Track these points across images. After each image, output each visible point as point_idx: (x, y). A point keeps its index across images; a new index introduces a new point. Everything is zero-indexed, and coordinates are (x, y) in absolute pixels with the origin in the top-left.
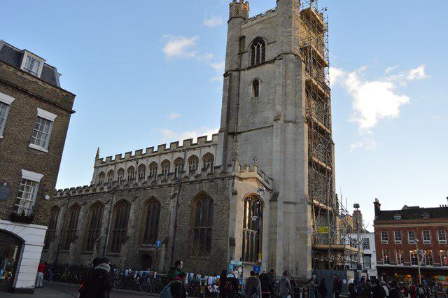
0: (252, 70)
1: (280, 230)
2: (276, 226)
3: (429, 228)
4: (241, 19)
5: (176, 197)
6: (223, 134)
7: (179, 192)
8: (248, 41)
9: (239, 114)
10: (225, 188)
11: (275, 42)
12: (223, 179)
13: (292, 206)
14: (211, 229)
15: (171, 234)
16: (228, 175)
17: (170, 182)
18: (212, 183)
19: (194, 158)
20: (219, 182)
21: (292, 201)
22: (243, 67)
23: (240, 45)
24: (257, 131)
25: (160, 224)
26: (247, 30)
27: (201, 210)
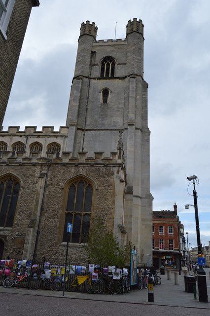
0: (102, 81)
1: (133, 219)
2: (131, 216)
5: (45, 178)
6: (74, 128)
7: (48, 172)
8: (99, 58)
9: (89, 113)
11: (125, 64)
14: (89, 215)
15: (38, 218)
16: (111, 162)
17: (34, 161)
18: (92, 168)
19: (37, 147)
20: (103, 170)
21: (140, 196)
23: (91, 57)
25: (19, 204)
27: (76, 194)
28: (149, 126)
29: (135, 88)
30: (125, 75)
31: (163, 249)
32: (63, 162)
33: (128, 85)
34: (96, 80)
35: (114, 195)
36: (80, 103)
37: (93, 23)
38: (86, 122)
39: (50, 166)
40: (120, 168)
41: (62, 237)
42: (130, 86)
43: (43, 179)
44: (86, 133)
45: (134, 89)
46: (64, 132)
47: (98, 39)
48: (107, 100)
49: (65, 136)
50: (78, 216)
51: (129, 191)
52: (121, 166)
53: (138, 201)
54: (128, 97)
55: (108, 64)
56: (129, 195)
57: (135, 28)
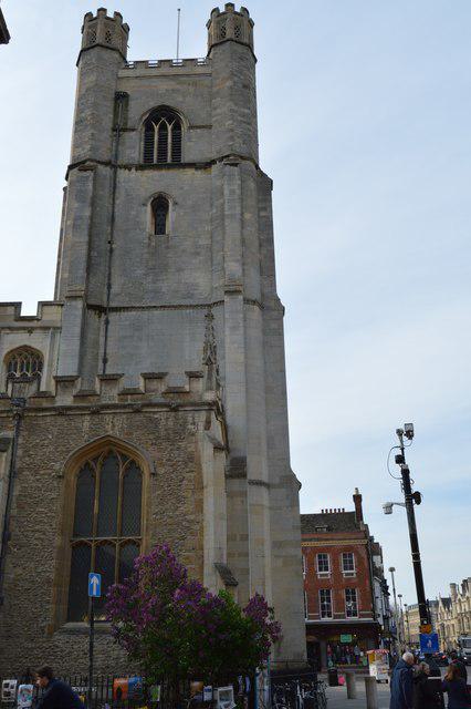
0: (149, 173)
1: (251, 545)
2: (245, 538)
3: (328, 549)
4: (117, 55)
6: (79, 304)
8: (137, 111)
9: (117, 262)
10: (181, 433)
12: (175, 410)
13: (264, 490)
18: (138, 417)
20: (164, 418)
21: (265, 479)
22: (119, 163)
24: (166, 312)
26: (133, 83)
27: (97, 490)
28: (280, 292)
29: (238, 192)
30: (214, 156)
31: (329, 616)
32: (58, 404)
33: (218, 183)
34: (133, 170)
35: (199, 487)
36: (90, 236)
37: (117, 14)
38: (109, 287)
39: (20, 417)
40: (213, 415)
41: (64, 607)
42: (225, 187)
43: (5, 454)
44: (113, 317)
45: (236, 197)
46: (53, 316)
47: (131, 57)
48: (164, 225)
49: (55, 328)
50: (106, 548)
51: (237, 470)
52: (217, 408)
53: (261, 497)
54: (223, 216)
55: (163, 128)
56: (237, 481)
57: (232, 32)
